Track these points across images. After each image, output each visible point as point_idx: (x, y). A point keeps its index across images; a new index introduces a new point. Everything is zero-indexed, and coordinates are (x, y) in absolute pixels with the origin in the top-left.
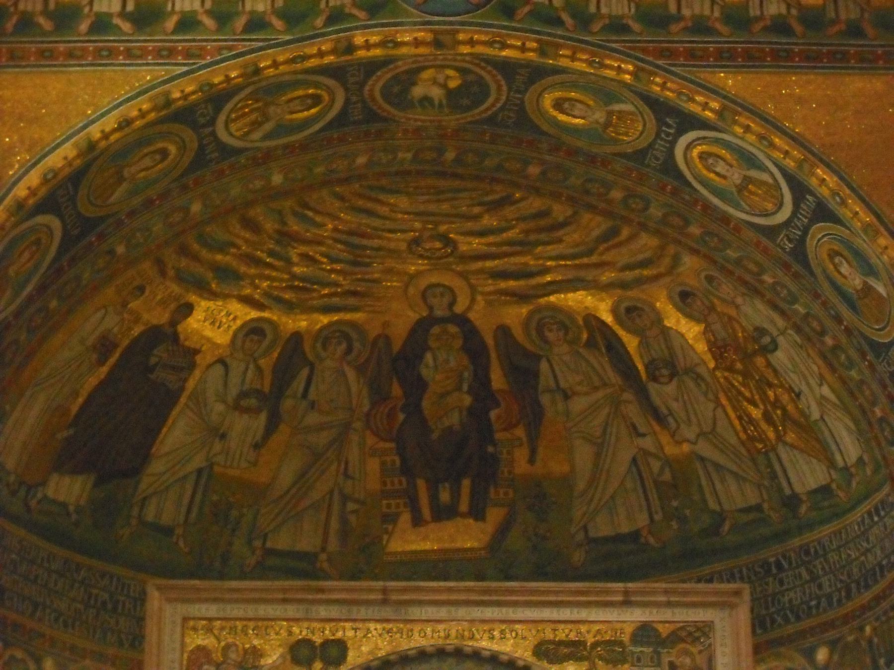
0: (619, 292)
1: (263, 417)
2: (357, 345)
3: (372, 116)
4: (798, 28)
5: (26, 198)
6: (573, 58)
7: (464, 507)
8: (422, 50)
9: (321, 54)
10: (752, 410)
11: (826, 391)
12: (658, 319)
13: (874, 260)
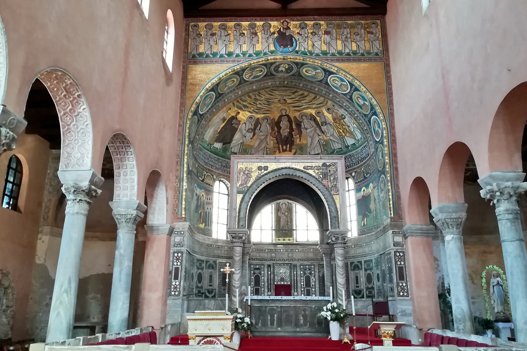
0: (316, 109)
1: (252, 133)
2: (269, 120)
3: (272, 74)
4: (352, 55)
5: (208, 88)
6: (309, 61)
7: (288, 150)
8: (281, 60)
9: (262, 61)
10: (340, 130)
11: (355, 125)
12: (323, 114)
13: (366, 98)
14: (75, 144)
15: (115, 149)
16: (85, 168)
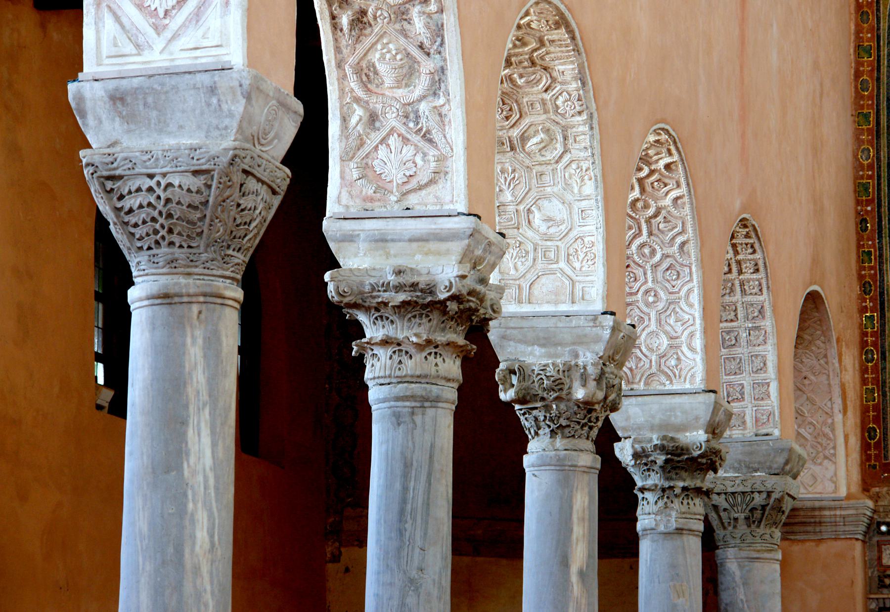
14: (648, 305)
16: (687, 386)
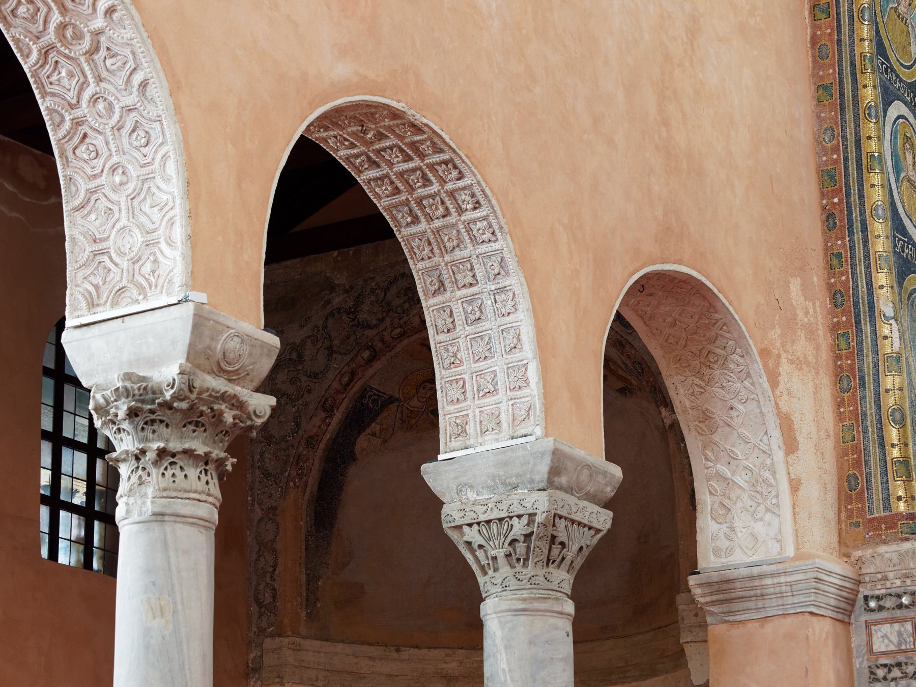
15: (397, 191)
